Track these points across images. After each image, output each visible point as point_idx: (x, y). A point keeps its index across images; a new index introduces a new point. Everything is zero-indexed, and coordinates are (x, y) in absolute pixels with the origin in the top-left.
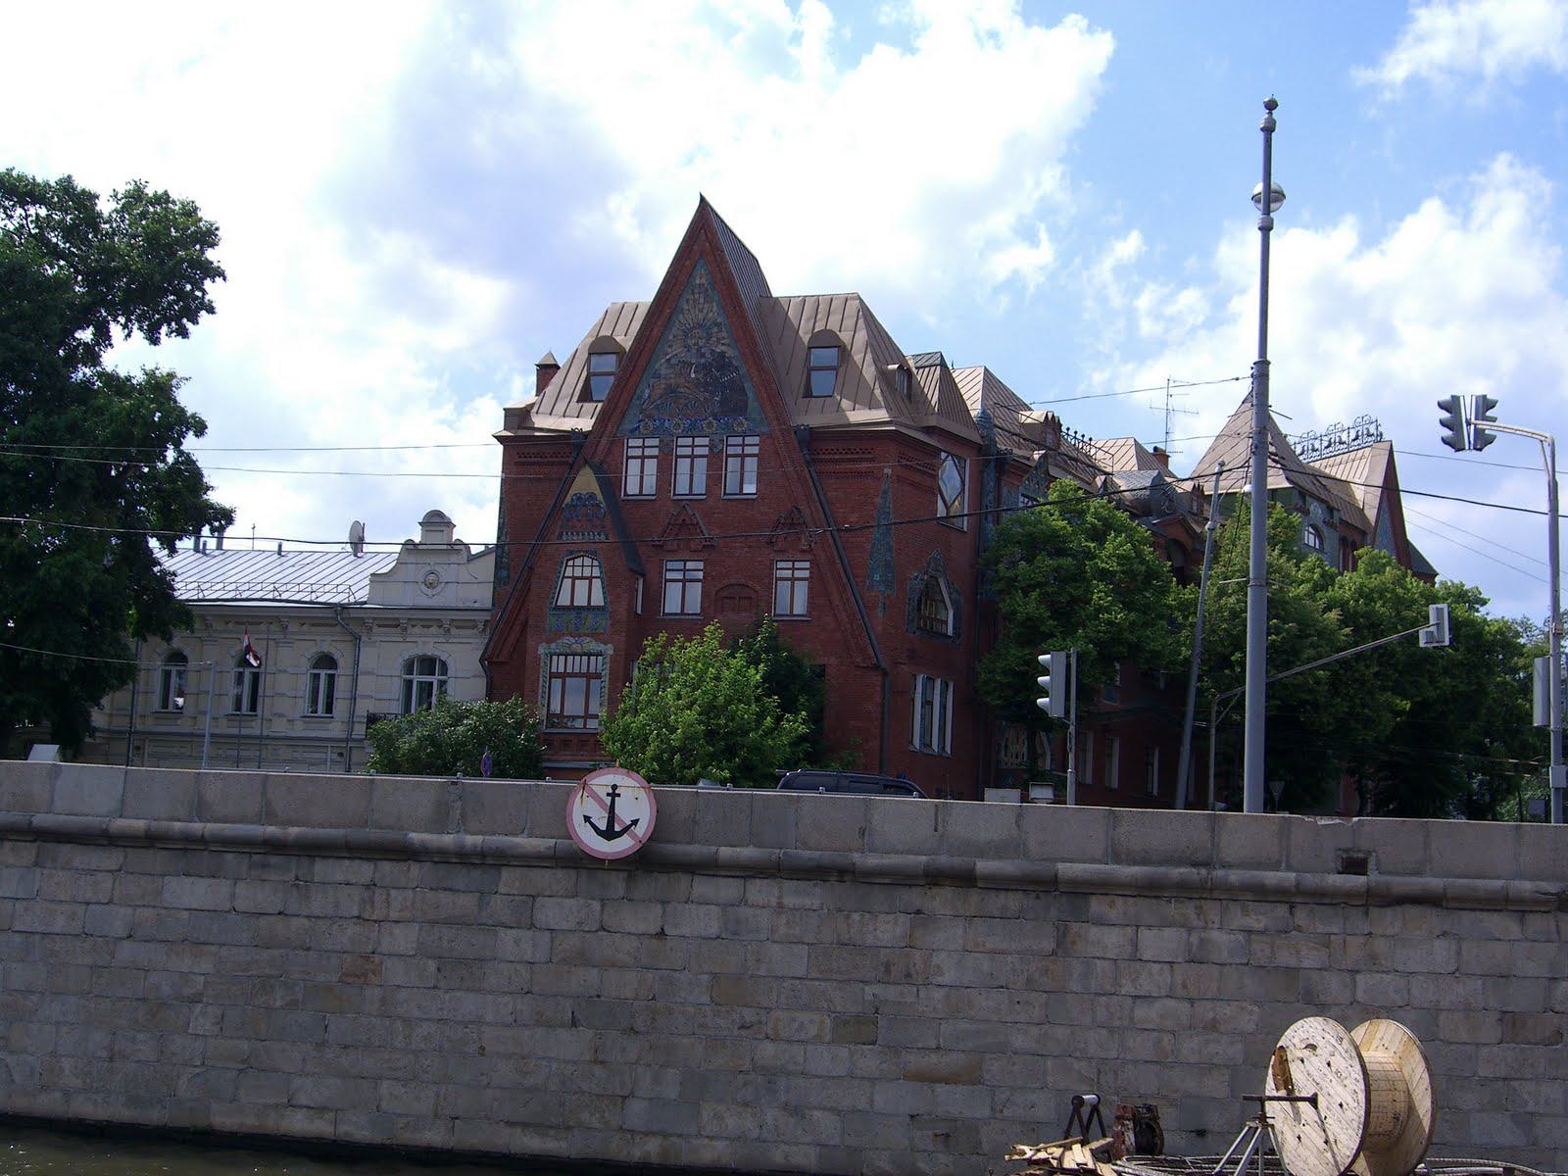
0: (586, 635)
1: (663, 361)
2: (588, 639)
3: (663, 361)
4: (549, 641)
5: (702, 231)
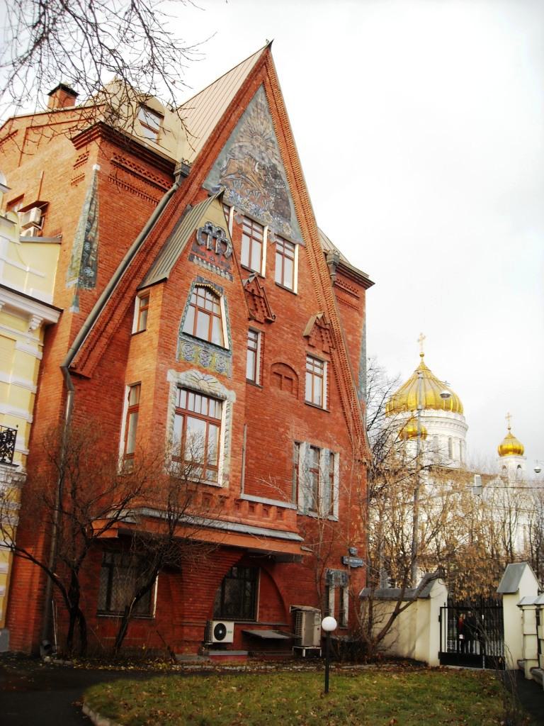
0: (213, 374)
1: (237, 145)
2: (215, 379)
3: (237, 145)
4: (179, 369)
5: (264, 67)
